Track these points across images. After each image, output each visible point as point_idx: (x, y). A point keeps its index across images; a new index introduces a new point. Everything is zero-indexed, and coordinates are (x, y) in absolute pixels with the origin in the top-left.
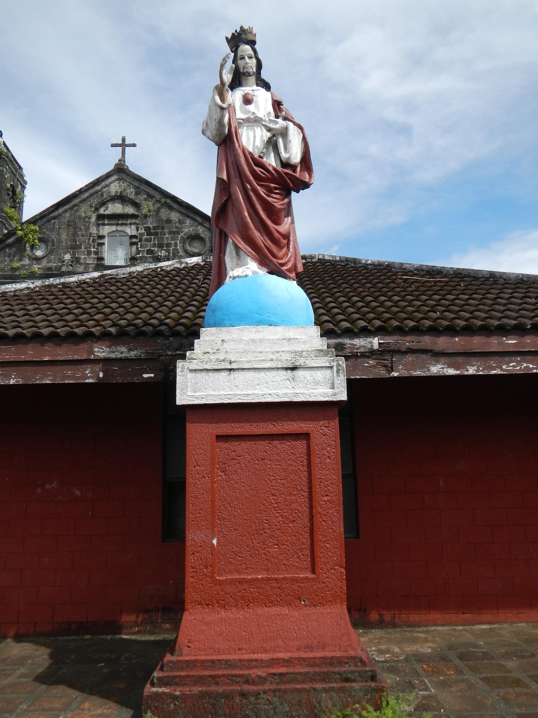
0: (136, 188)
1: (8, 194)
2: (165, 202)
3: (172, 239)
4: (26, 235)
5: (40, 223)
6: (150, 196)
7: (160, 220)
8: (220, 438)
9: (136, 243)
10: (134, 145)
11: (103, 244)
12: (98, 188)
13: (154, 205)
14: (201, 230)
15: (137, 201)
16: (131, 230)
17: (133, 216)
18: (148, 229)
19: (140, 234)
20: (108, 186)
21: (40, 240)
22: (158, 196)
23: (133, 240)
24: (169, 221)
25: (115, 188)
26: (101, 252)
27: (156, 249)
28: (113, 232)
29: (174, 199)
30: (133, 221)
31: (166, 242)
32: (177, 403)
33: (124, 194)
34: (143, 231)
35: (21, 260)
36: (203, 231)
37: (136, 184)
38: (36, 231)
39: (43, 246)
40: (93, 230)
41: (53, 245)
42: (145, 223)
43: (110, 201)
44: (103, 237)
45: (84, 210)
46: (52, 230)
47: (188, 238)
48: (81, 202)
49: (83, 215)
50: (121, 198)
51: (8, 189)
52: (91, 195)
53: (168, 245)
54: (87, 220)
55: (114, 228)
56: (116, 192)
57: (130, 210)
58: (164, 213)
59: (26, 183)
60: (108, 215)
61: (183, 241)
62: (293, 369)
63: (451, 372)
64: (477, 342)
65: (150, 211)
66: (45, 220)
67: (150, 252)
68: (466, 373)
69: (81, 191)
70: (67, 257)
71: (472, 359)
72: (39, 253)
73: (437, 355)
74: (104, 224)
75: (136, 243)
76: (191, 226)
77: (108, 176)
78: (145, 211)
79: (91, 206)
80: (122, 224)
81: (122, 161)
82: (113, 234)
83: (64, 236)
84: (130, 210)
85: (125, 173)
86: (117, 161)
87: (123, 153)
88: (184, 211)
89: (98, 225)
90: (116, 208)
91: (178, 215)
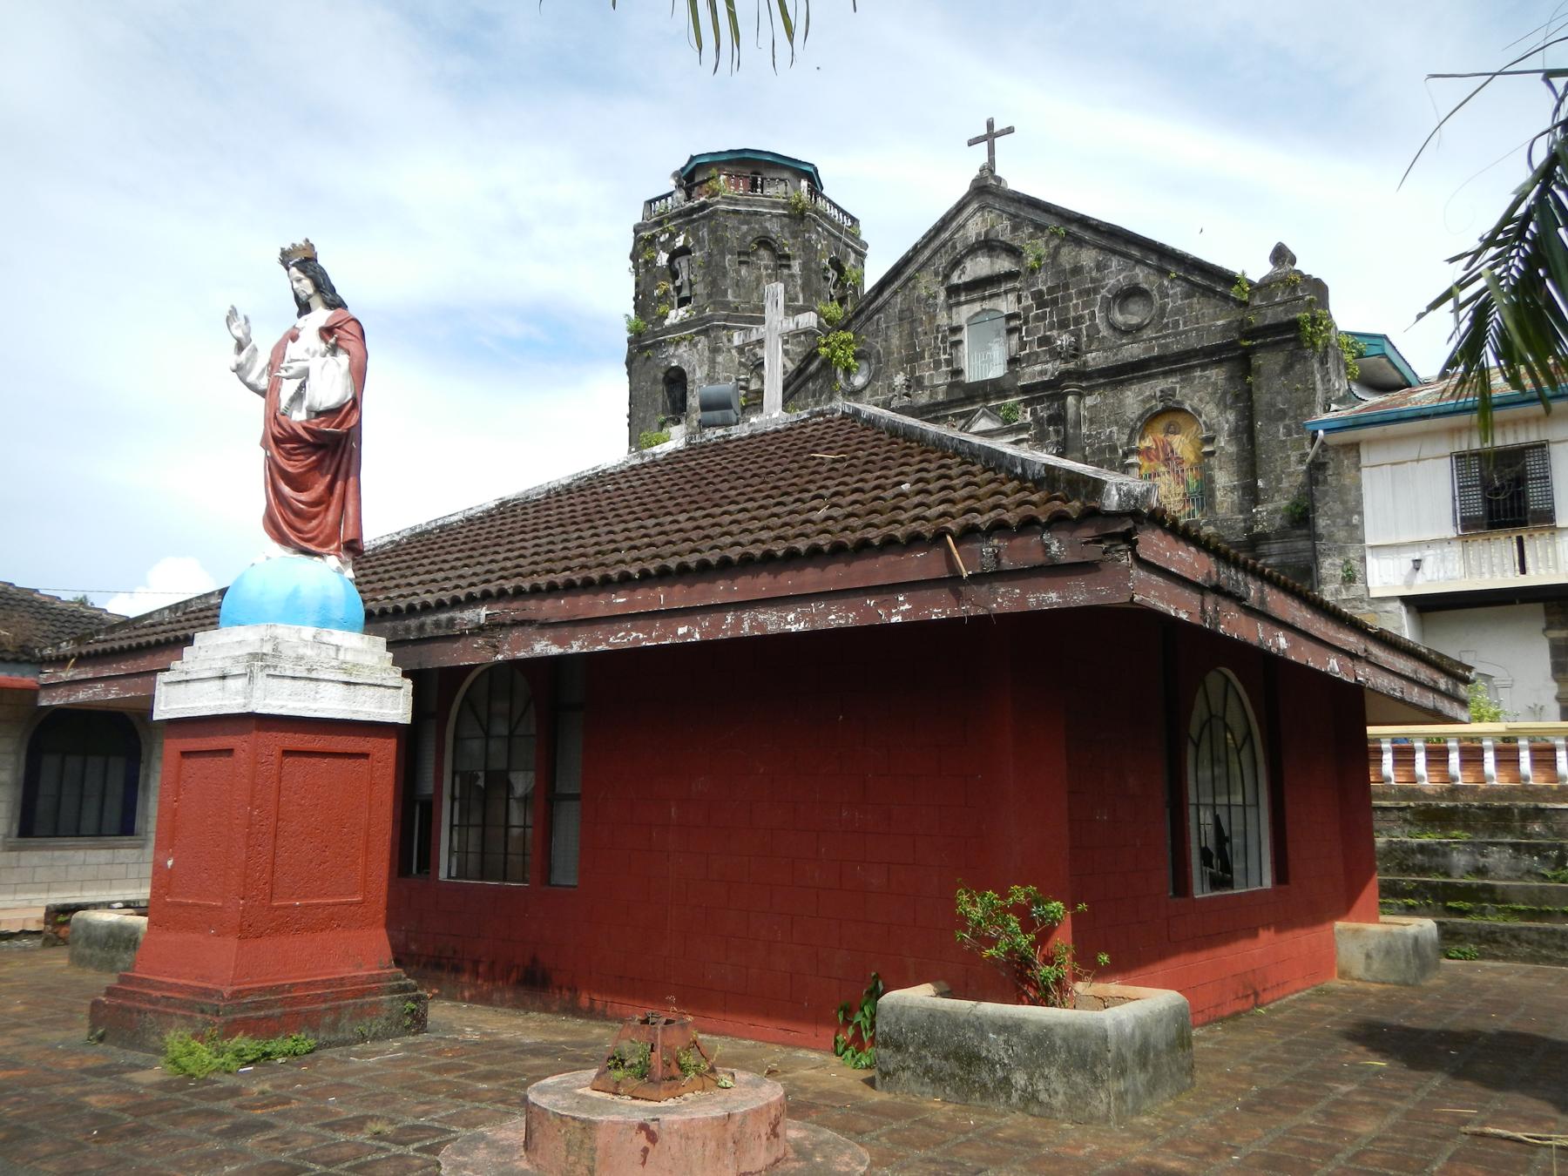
0: (1013, 217)
1: (827, 279)
2: (1067, 233)
3: (1086, 305)
4: (834, 352)
5: (856, 324)
6: (1040, 228)
7: (1060, 272)
8: (185, 754)
9: (1017, 329)
10: (1010, 130)
11: (960, 342)
12: (945, 235)
13: (1047, 243)
14: (1141, 275)
15: (1016, 243)
16: (1007, 305)
17: (1010, 276)
18: (1038, 296)
19: (1025, 309)
20: (963, 226)
21: (857, 356)
22: (1053, 223)
23: (1013, 325)
24: (1077, 270)
25: (975, 227)
26: (958, 359)
27: (1055, 333)
28: (977, 314)
29: (1083, 221)
30: (1010, 285)
31: (1072, 314)
32: (156, 717)
33: (992, 236)
34: (1030, 302)
35: (831, 399)
36: (1146, 277)
37: (1012, 210)
38: (848, 343)
39: (865, 366)
40: (943, 319)
41: (879, 362)
42: (1033, 285)
43: (967, 254)
44: (956, 330)
45: (928, 284)
46: (876, 334)
47: (1115, 297)
48: (918, 270)
49: (924, 293)
50: (987, 245)
51: (826, 269)
52: (935, 252)
53: (1078, 320)
54: (931, 301)
55: (977, 307)
56: (979, 235)
57: (1004, 264)
58: (1067, 256)
59: (866, 246)
60: (966, 284)
61: (1107, 306)
62: (224, 677)
63: (555, 650)
64: (585, 605)
65: (1039, 259)
66: (863, 317)
67: (1044, 341)
68: (570, 651)
69: (916, 250)
70: (899, 379)
71: (578, 629)
72: (859, 381)
73: (545, 625)
74: (959, 304)
75: (1017, 329)
76: (1120, 271)
77: (960, 207)
78: (1031, 261)
79: (937, 274)
80: (991, 296)
81: (990, 168)
82: (977, 319)
83: (895, 341)
84: (1004, 264)
85: (990, 193)
86: (975, 173)
87: (991, 151)
88: (1104, 242)
89: (950, 307)
90: (979, 267)
91: (1094, 253)
